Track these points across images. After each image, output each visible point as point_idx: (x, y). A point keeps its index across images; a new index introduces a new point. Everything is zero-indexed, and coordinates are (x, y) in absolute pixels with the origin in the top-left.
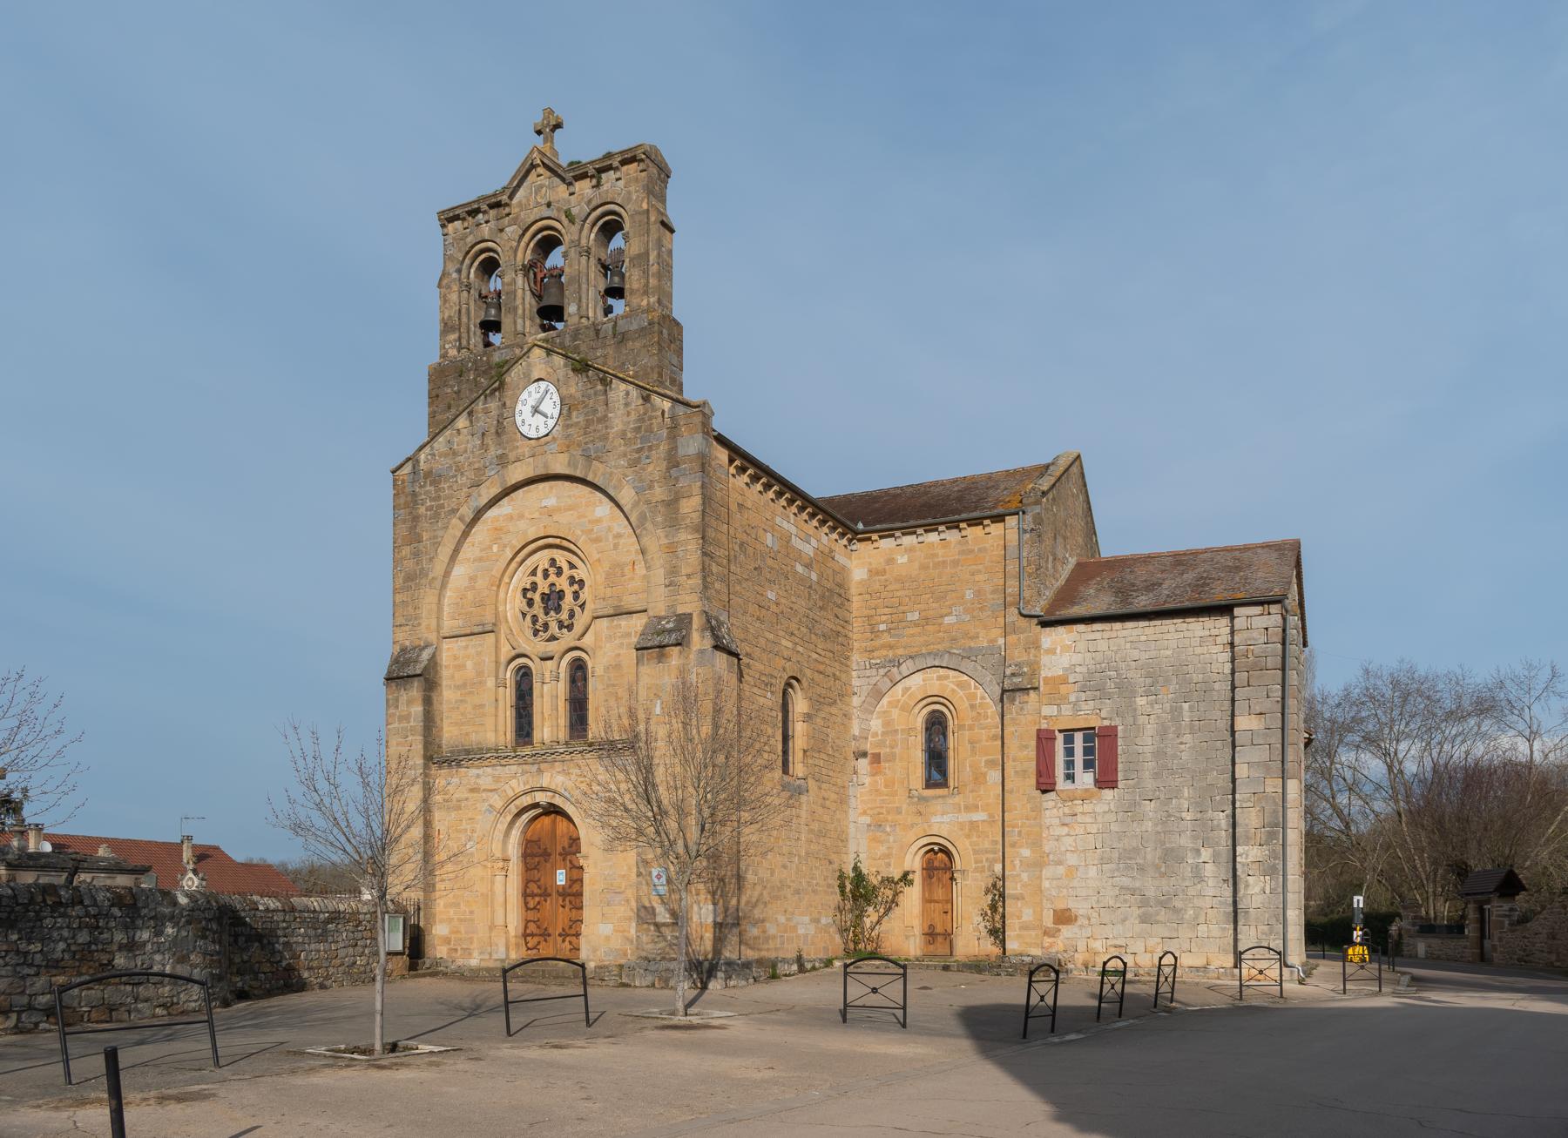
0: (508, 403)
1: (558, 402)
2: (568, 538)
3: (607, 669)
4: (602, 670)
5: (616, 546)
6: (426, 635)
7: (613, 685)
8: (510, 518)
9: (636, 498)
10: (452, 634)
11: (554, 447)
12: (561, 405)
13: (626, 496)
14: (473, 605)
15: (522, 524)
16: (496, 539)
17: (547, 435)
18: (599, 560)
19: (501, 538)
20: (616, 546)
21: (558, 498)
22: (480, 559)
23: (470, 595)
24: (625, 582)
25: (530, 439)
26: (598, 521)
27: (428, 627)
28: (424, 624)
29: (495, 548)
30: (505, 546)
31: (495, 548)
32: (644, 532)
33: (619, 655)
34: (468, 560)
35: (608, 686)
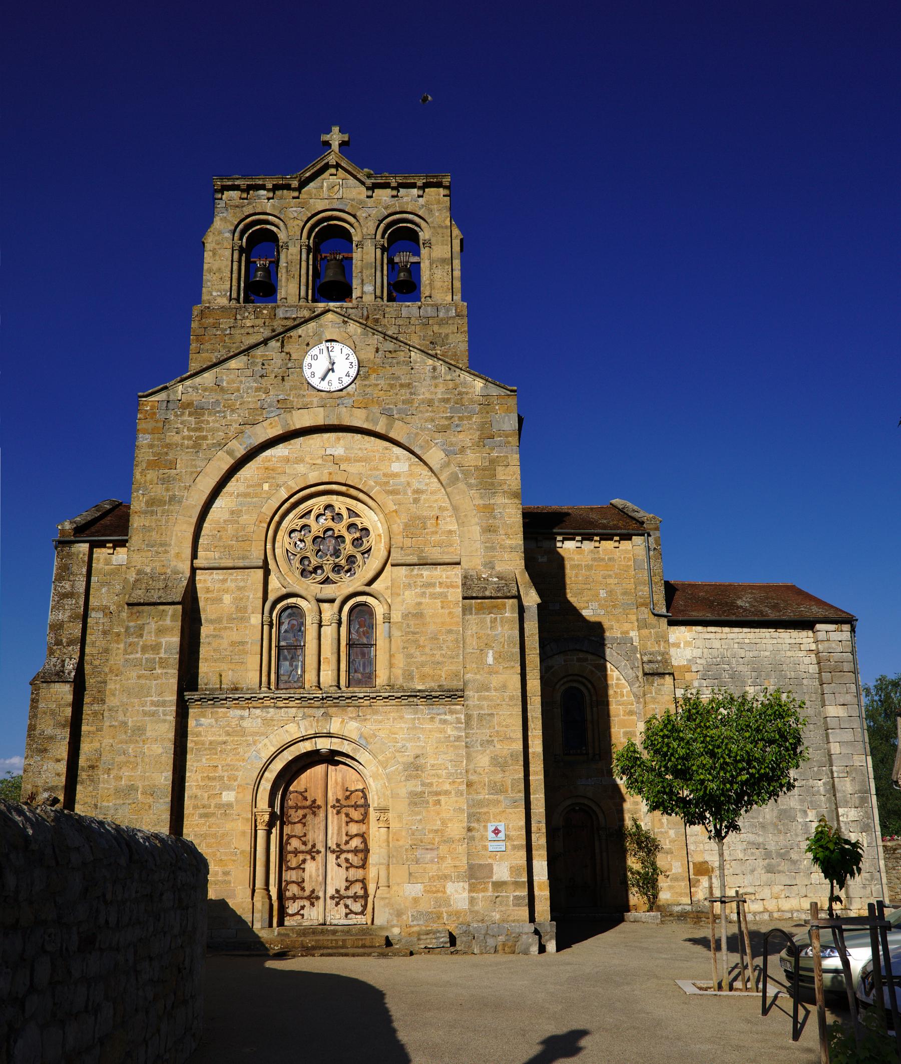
0: (294, 356)
1: (355, 362)
2: (360, 487)
3: (405, 616)
4: (400, 616)
5: (416, 501)
6: (173, 563)
7: (414, 633)
8: (287, 460)
9: (446, 459)
10: (207, 565)
11: (349, 401)
12: (359, 367)
13: (435, 456)
14: (235, 539)
15: (301, 468)
16: (269, 478)
17: (341, 390)
18: (396, 511)
19: (273, 478)
20: (416, 501)
21: (346, 449)
22: (246, 495)
23: (230, 529)
24: (427, 534)
25: (319, 390)
26: (396, 475)
27: (178, 555)
28: (173, 552)
29: (266, 487)
30: (279, 486)
31: (266, 487)
32: (455, 491)
33: (420, 604)
34: (231, 495)
35: (408, 633)
